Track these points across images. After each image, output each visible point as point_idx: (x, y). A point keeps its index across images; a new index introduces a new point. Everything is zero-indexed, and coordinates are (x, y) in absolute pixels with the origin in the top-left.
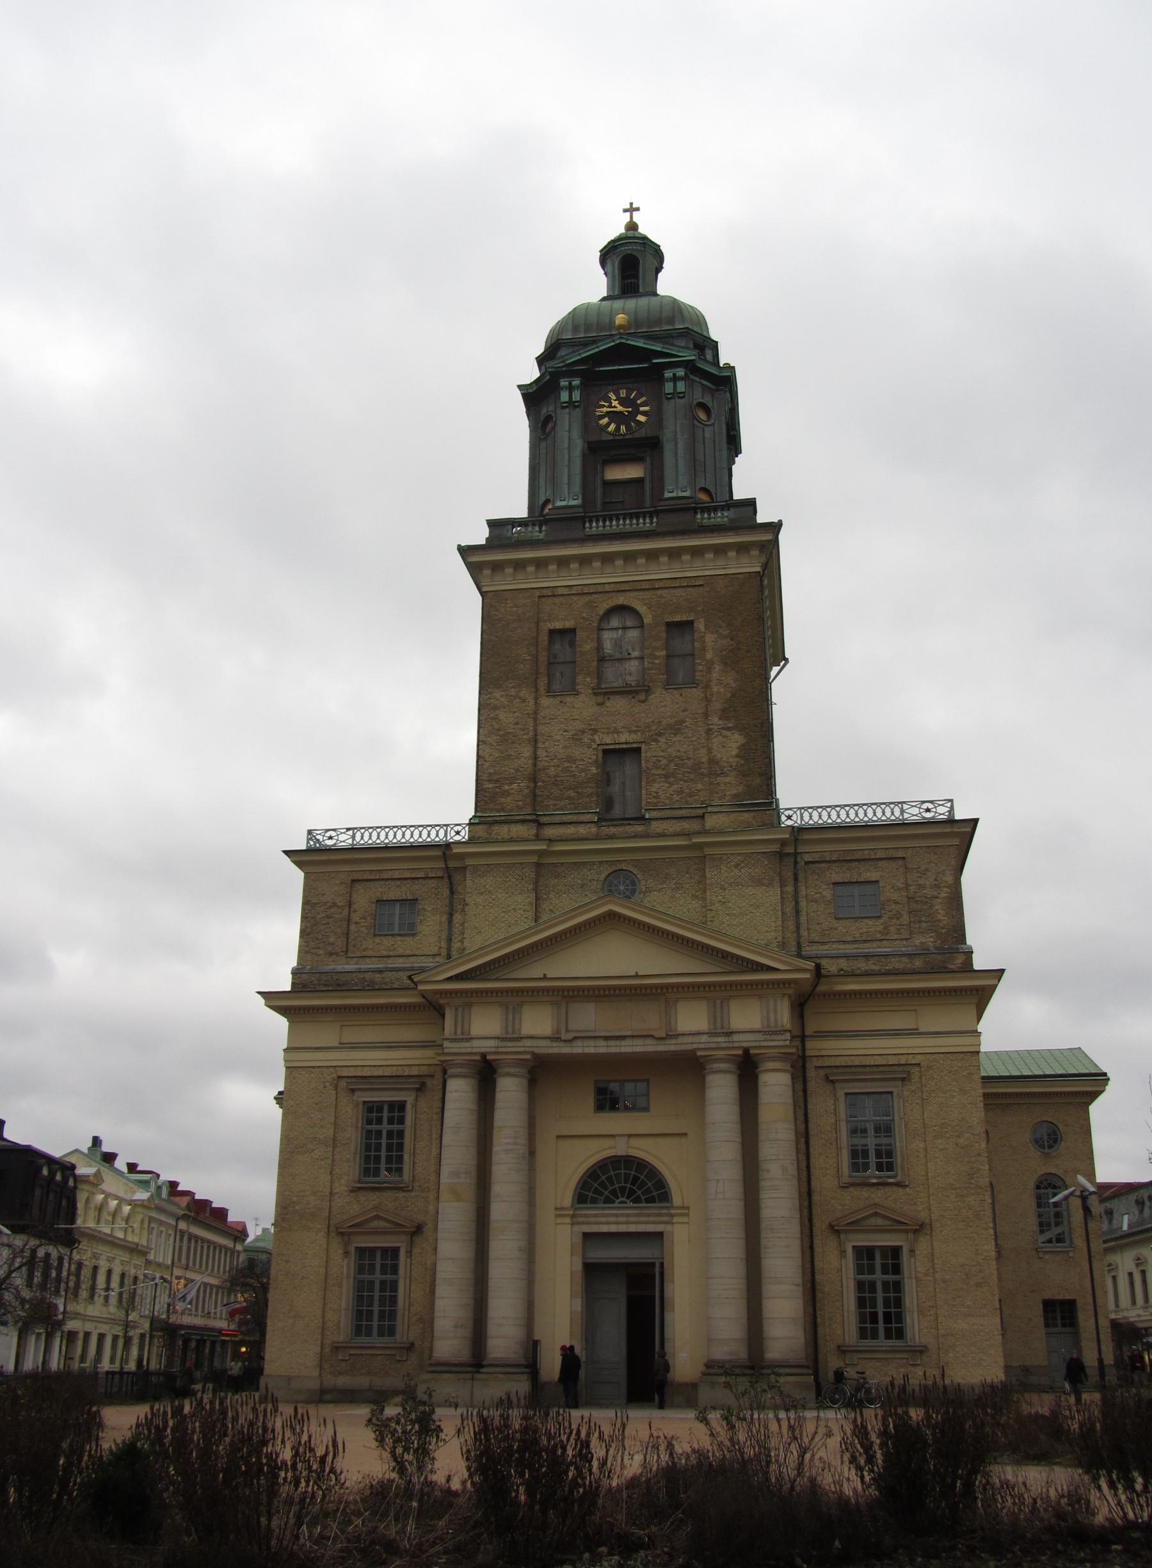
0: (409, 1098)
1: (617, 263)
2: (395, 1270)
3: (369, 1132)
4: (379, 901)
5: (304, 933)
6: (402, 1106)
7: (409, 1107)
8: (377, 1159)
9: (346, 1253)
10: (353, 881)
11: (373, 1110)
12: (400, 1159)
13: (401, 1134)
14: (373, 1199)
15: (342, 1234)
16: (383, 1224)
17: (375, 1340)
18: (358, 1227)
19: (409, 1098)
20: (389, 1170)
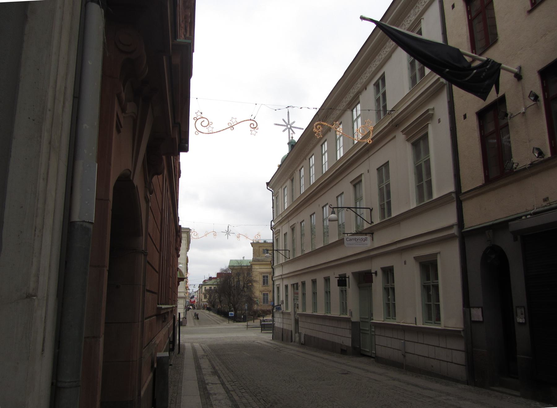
0: (269, 275)
1: (291, 146)
2: (268, 296)
3: (263, 280)
4: (263, 250)
5: (253, 254)
6: (268, 276)
7: (269, 276)
8: (265, 283)
9: (262, 294)
10: (260, 247)
11: (264, 277)
12: (268, 283)
13: (268, 279)
14: (265, 287)
15: (261, 292)
16: (266, 291)
17: (266, 304)
18: (263, 291)
19: (269, 275)
20: (266, 284)
